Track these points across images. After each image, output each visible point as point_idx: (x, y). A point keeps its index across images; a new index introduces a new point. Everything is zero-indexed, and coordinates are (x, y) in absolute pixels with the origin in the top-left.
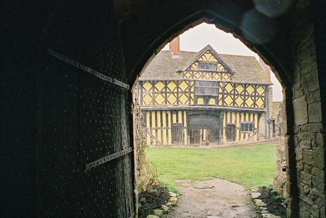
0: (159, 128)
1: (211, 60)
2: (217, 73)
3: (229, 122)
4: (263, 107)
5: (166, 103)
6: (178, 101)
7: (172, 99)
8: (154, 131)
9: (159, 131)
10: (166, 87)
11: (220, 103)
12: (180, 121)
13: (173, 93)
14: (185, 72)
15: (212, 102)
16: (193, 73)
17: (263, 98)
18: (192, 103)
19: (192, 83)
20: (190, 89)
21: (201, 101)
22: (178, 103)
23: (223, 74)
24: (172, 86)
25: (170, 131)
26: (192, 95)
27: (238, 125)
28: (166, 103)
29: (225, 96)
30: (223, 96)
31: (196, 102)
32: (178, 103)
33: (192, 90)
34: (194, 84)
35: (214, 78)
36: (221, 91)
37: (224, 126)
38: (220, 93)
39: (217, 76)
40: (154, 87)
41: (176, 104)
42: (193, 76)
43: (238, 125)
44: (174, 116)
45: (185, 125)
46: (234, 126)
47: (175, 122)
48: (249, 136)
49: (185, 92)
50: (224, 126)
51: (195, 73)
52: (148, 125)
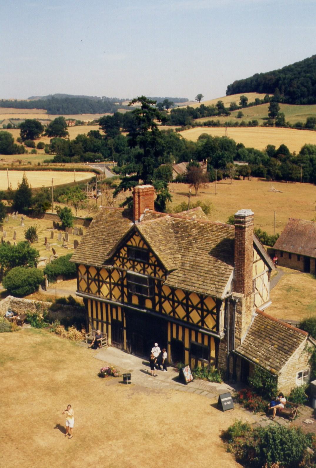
0: (100, 321)
1: (141, 246)
2: (150, 265)
3: (174, 336)
4: (215, 330)
5: (99, 294)
6: (110, 293)
7: (105, 290)
8: (95, 323)
9: (100, 324)
10: (98, 274)
11: (157, 308)
12: (120, 319)
13: (106, 283)
14: (115, 258)
15: (149, 304)
16: (123, 260)
17: (215, 317)
18: (126, 300)
19: (125, 274)
20: (122, 283)
21: (135, 300)
22: (111, 297)
23: (158, 268)
24: (104, 275)
25: (110, 326)
26: (125, 290)
27: (187, 345)
28: (99, 294)
29: (163, 300)
30: (160, 299)
31: (130, 300)
32: (111, 297)
33: (125, 282)
34: (126, 277)
35: (146, 273)
36: (157, 292)
37: (169, 340)
38: (156, 294)
39: (149, 270)
40: (88, 272)
41: (109, 297)
42: (123, 264)
43: (187, 345)
44: (114, 311)
45: (125, 326)
46: (182, 344)
47: (114, 317)
48: (203, 365)
49: (116, 284)
50: (169, 340)
51: (125, 261)
52: (90, 315)
